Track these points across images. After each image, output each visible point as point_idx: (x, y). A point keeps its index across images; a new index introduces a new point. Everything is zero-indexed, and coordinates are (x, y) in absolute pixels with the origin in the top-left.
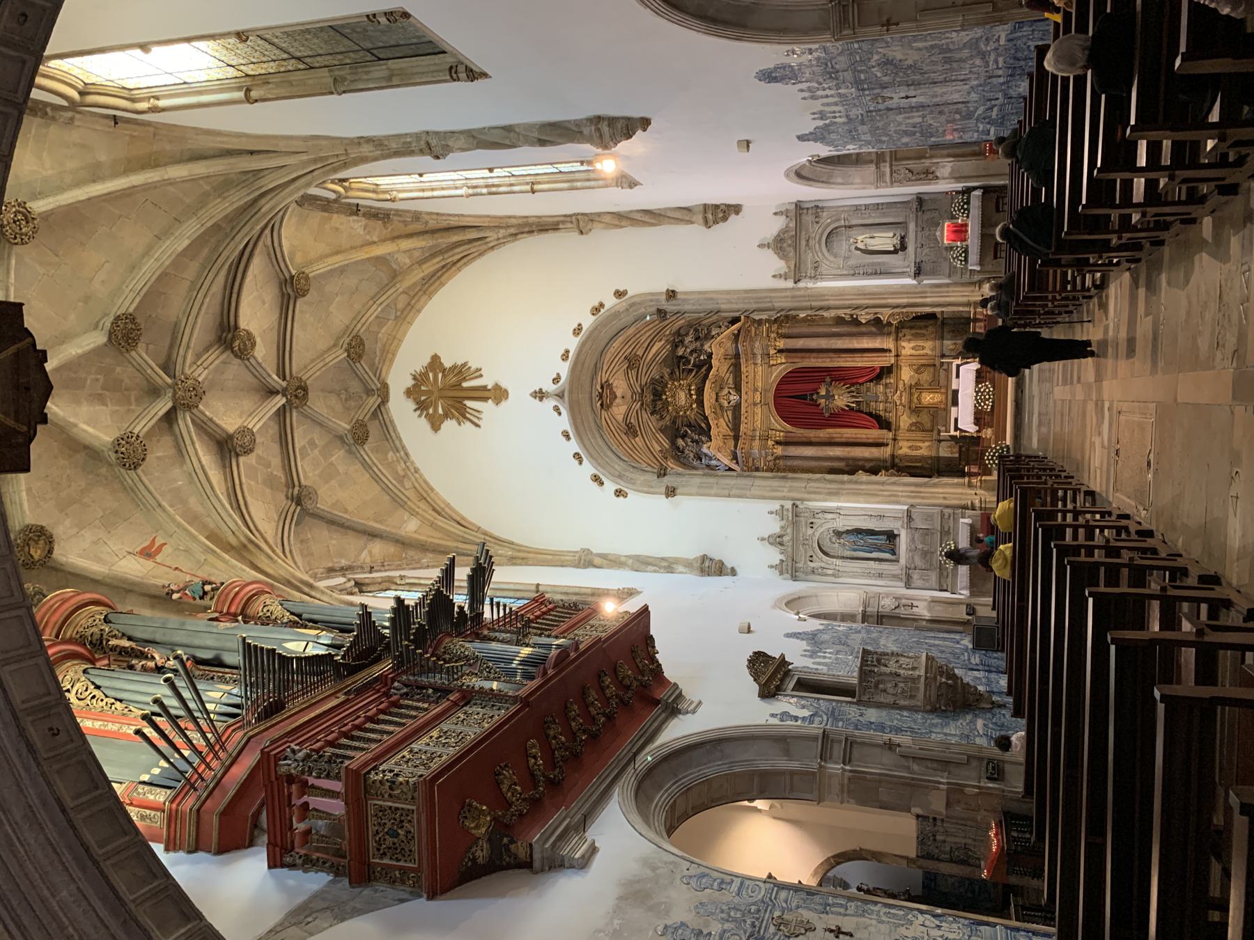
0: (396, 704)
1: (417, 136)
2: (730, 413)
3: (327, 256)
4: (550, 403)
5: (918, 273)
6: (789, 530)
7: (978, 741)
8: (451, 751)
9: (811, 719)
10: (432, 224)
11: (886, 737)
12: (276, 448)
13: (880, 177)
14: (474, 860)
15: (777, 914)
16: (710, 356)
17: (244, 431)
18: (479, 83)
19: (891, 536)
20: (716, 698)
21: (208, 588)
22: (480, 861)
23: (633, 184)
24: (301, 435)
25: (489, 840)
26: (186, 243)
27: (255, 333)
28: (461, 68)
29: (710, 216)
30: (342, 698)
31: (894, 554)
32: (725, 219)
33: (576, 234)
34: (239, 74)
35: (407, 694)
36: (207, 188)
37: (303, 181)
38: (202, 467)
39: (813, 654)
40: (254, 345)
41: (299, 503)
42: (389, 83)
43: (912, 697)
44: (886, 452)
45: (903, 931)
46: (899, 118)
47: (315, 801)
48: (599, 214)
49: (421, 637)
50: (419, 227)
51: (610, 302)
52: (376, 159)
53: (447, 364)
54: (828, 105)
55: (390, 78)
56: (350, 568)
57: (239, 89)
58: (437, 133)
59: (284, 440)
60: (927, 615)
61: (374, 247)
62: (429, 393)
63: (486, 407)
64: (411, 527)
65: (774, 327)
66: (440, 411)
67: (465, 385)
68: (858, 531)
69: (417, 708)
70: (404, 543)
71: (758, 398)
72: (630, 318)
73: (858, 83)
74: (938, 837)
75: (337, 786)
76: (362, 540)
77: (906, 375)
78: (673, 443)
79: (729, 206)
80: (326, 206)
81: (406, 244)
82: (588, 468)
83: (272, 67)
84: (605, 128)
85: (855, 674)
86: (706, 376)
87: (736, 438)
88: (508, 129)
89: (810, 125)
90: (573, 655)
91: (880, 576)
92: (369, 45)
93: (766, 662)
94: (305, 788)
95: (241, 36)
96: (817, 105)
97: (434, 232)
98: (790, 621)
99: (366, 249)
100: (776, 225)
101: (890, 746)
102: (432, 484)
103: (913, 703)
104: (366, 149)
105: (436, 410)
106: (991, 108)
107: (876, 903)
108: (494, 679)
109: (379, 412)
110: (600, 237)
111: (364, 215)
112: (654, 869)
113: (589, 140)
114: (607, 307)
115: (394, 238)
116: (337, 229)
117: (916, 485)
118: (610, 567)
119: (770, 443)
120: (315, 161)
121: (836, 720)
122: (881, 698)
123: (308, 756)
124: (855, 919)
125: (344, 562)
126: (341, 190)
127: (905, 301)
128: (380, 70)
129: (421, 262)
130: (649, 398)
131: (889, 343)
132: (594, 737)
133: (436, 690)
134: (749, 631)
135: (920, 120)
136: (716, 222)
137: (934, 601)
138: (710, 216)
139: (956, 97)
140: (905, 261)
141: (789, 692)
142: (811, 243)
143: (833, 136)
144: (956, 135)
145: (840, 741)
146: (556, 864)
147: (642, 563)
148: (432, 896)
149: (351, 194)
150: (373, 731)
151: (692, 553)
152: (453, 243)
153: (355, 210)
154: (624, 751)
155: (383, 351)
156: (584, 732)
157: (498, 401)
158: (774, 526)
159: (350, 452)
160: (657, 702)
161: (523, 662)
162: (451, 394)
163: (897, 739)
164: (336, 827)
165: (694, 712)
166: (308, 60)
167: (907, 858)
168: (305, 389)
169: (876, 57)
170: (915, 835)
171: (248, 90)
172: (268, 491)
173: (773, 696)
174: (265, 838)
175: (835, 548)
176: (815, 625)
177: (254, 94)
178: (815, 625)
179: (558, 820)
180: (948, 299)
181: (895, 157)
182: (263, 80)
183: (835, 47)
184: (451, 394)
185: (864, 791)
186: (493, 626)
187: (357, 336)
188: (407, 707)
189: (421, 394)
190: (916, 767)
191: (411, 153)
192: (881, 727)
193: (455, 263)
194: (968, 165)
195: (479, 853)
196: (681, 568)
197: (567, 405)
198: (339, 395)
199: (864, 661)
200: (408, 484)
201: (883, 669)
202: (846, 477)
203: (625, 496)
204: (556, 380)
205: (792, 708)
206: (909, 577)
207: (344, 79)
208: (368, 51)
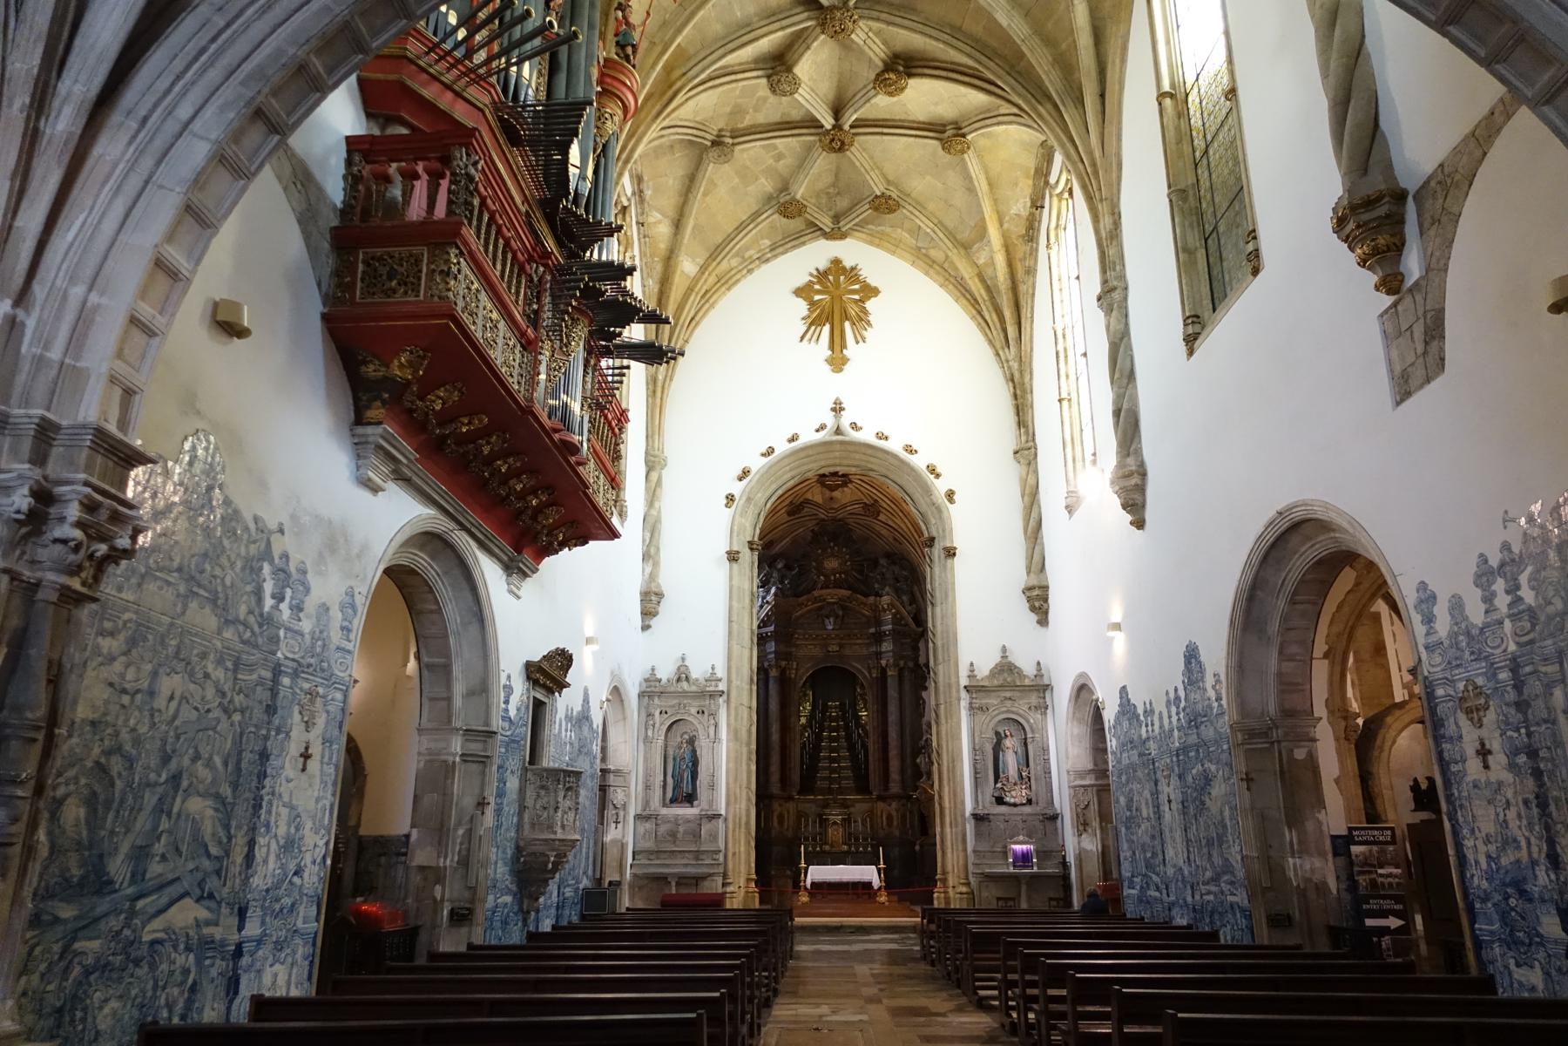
0: (522, 269)
1: (1122, 277)
3: (986, 173)
4: (829, 420)
5: (978, 818)
6: (694, 688)
7: (491, 898)
8: (479, 335)
9: (506, 718)
10: (1022, 288)
11: (492, 800)
12: (775, 117)
13: (1081, 774)
14: (365, 363)
15: (321, 690)
17: (796, 83)
18: (1182, 347)
19: (690, 798)
21: (629, 50)
22: (363, 369)
23: (1070, 509)
24: (788, 145)
25: (385, 378)
26: (1004, 22)
27: (902, 96)
28: (1197, 328)
29: (1036, 592)
30: (523, 209)
31: (672, 801)
32: (1033, 609)
33: (1014, 447)
34: (1189, 86)
35: (531, 281)
36: (1064, 46)
37: (1072, 151)
38: (757, 39)
39: (569, 718)
40: (891, 94)
41: (715, 143)
42: (1183, 251)
43: (533, 825)
45: (309, 825)
46: (1147, 794)
47: (420, 188)
48: (1036, 472)
49: (591, 294)
50: (1020, 274)
52: (1097, 231)
53: (869, 305)
54: (1161, 718)
55: (1185, 250)
56: (642, 200)
57: (1173, 85)
58: (1126, 298)
59: (785, 126)
60: (608, 838)
61: (997, 225)
62: (837, 284)
64: (687, 266)
65: (911, 664)
66: (817, 297)
67: (847, 324)
68: (695, 762)
69: (518, 293)
70: (669, 260)
71: (836, 648)
72: (924, 507)
73: (1184, 749)
74: (383, 860)
75: (440, 211)
76: (671, 212)
78: (780, 555)
79: (1046, 613)
80: (1042, 172)
81: (1000, 260)
82: (757, 464)
83: (1196, 121)
84: (1135, 480)
85: (551, 764)
86: (855, 591)
88: (1131, 376)
89: (1138, 699)
90: (573, 459)
91: (647, 787)
92: (1221, 229)
93: (561, 668)
95: (1231, 94)
96: (1160, 706)
98: (600, 694)
99: (995, 217)
101: (482, 804)
103: (527, 827)
104: (1106, 222)
105: (818, 292)
106: (1158, 889)
107: (334, 795)
108: (548, 375)
109: (815, 230)
110: (1011, 472)
111: (1032, 214)
112: (359, 556)
113: (1121, 465)
115: (1008, 249)
116: (1016, 184)
117: (747, 823)
118: (647, 489)
120: (1094, 165)
121: (507, 745)
122: (530, 793)
123: (471, 179)
124: (318, 773)
125: (648, 193)
126: (1058, 190)
127: (947, 804)
128: (1194, 240)
129: (981, 277)
131: (895, 788)
133: (536, 312)
135: (1145, 814)
136: (1029, 599)
137: (623, 846)
138: (1036, 592)
139: (1170, 853)
141: (533, 693)
142: (1008, 703)
143: (1126, 724)
144: (1128, 854)
145: (485, 750)
146: (359, 448)
147: (652, 526)
148: (325, 318)
149: (1055, 200)
150: (496, 246)
151: (666, 582)
152: (1003, 311)
153: (1037, 205)
154: (472, 518)
155: (883, 233)
156: (491, 475)
158: (698, 672)
159: (770, 198)
160: (519, 552)
161: (565, 406)
162: (836, 307)
163: (490, 811)
164: (394, 210)
165: (511, 592)
166: (1205, 161)
167: (358, 825)
168: (841, 149)
169: (1213, 768)
170: (385, 833)
171: (1171, 96)
172: (728, 109)
173: (528, 678)
174: (376, 132)
175: (676, 739)
176: (597, 720)
177: (1168, 102)
178: (597, 720)
179: (406, 451)
180: (949, 851)
181: (1103, 791)
182: (1183, 113)
183: (1224, 725)
184: (836, 307)
186: (596, 368)
187: (899, 205)
188: (519, 283)
189: (836, 277)
190: (461, 832)
191: (1104, 270)
192: (501, 794)
193: (980, 313)
194: (1093, 867)
195: (371, 367)
196: (648, 570)
197: (828, 438)
198: (833, 185)
199: (568, 773)
200: (734, 262)
202: (754, 747)
204: (854, 426)
205: (516, 695)
206: (648, 818)
207: (1185, 200)
208: (1215, 228)
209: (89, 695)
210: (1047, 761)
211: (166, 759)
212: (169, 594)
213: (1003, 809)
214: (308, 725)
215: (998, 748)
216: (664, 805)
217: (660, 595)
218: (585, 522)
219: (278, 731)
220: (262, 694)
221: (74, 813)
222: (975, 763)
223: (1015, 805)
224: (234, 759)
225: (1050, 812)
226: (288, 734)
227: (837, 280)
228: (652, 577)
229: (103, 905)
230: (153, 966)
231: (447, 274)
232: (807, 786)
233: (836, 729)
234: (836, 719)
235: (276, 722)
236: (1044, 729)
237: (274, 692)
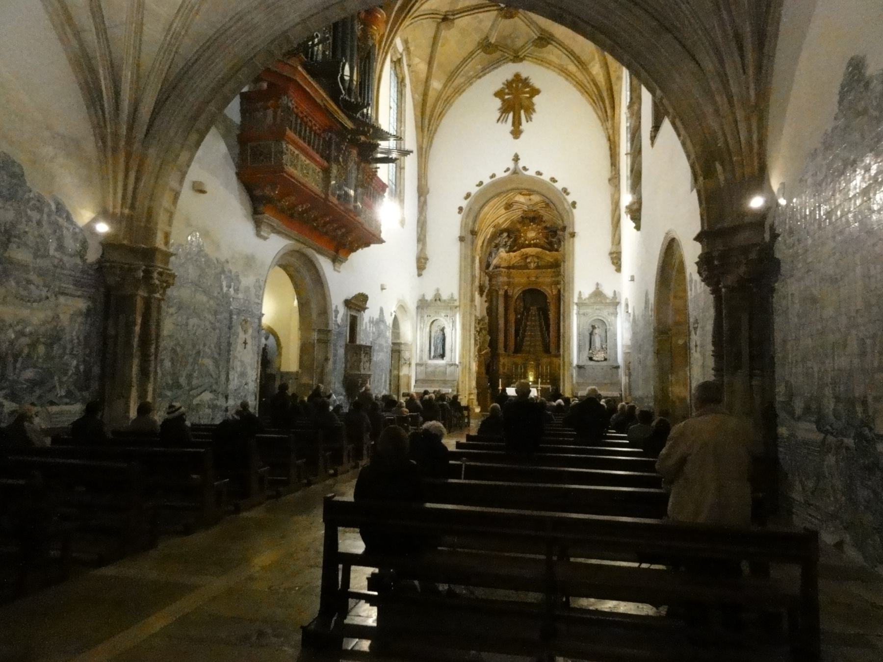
2: (523, 264)
4: (511, 165)
5: (579, 367)
10: (615, 88)
16: (557, 250)
20: (342, 280)
30: (322, 104)
32: (613, 263)
44: (501, 350)
50: (613, 79)
51: (570, 199)
53: (535, 99)
60: (402, 374)
63: (509, 126)
64: (436, 85)
66: (507, 97)
67: (522, 112)
68: (444, 340)
71: (534, 279)
77: (545, 360)
82: (474, 190)
84: (635, 207)
87: (508, 268)
91: (422, 351)
94: (276, 107)
97: (611, 90)
100: (608, 292)
102: (464, 94)
105: (508, 94)
114: (567, 197)
118: (419, 207)
119: (506, 287)
125: (412, 49)
130: (531, 215)
132: (316, 228)
133: (329, 155)
134: (383, 289)
136: (612, 258)
137: (409, 378)
140: (585, 362)
141: (349, 313)
142: (598, 311)
146: (258, 224)
148: (237, 174)
151: (430, 251)
157: (512, 132)
158: (445, 296)
160: (337, 251)
162: (517, 102)
165: (335, 270)
175: (435, 328)
176: (389, 321)
179: (275, 222)
185: (305, 349)
190: (319, 370)
192: (335, 355)
201: (363, 356)
203: (459, 213)
204: (525, 168)
205: (340, 315)
209: (168, 326)
210: (616, 340)
211: (194, 346)
212: (188, 291)
213: (592, 363)
214: (245, 332)
215: (591, 334)
216: (430, 359)
217: (426, 259)
218: (368, 237)
219: (234, 334)
220: (226, 322)
221: (167, 364)
222: (579, 341)
223: (598, 361)
224: (219, 345)
225: (615, 365)
226: (238, 336)
227: (517, 86)
228: (422, 250)
229: (180, 392)
230: (197, 412)
231: (282, 153)
232: (518, 349)
233: (535, 321)
234: (535, 316)
235: (233, 331)
236: (614, 325)
237: (231, 322)
